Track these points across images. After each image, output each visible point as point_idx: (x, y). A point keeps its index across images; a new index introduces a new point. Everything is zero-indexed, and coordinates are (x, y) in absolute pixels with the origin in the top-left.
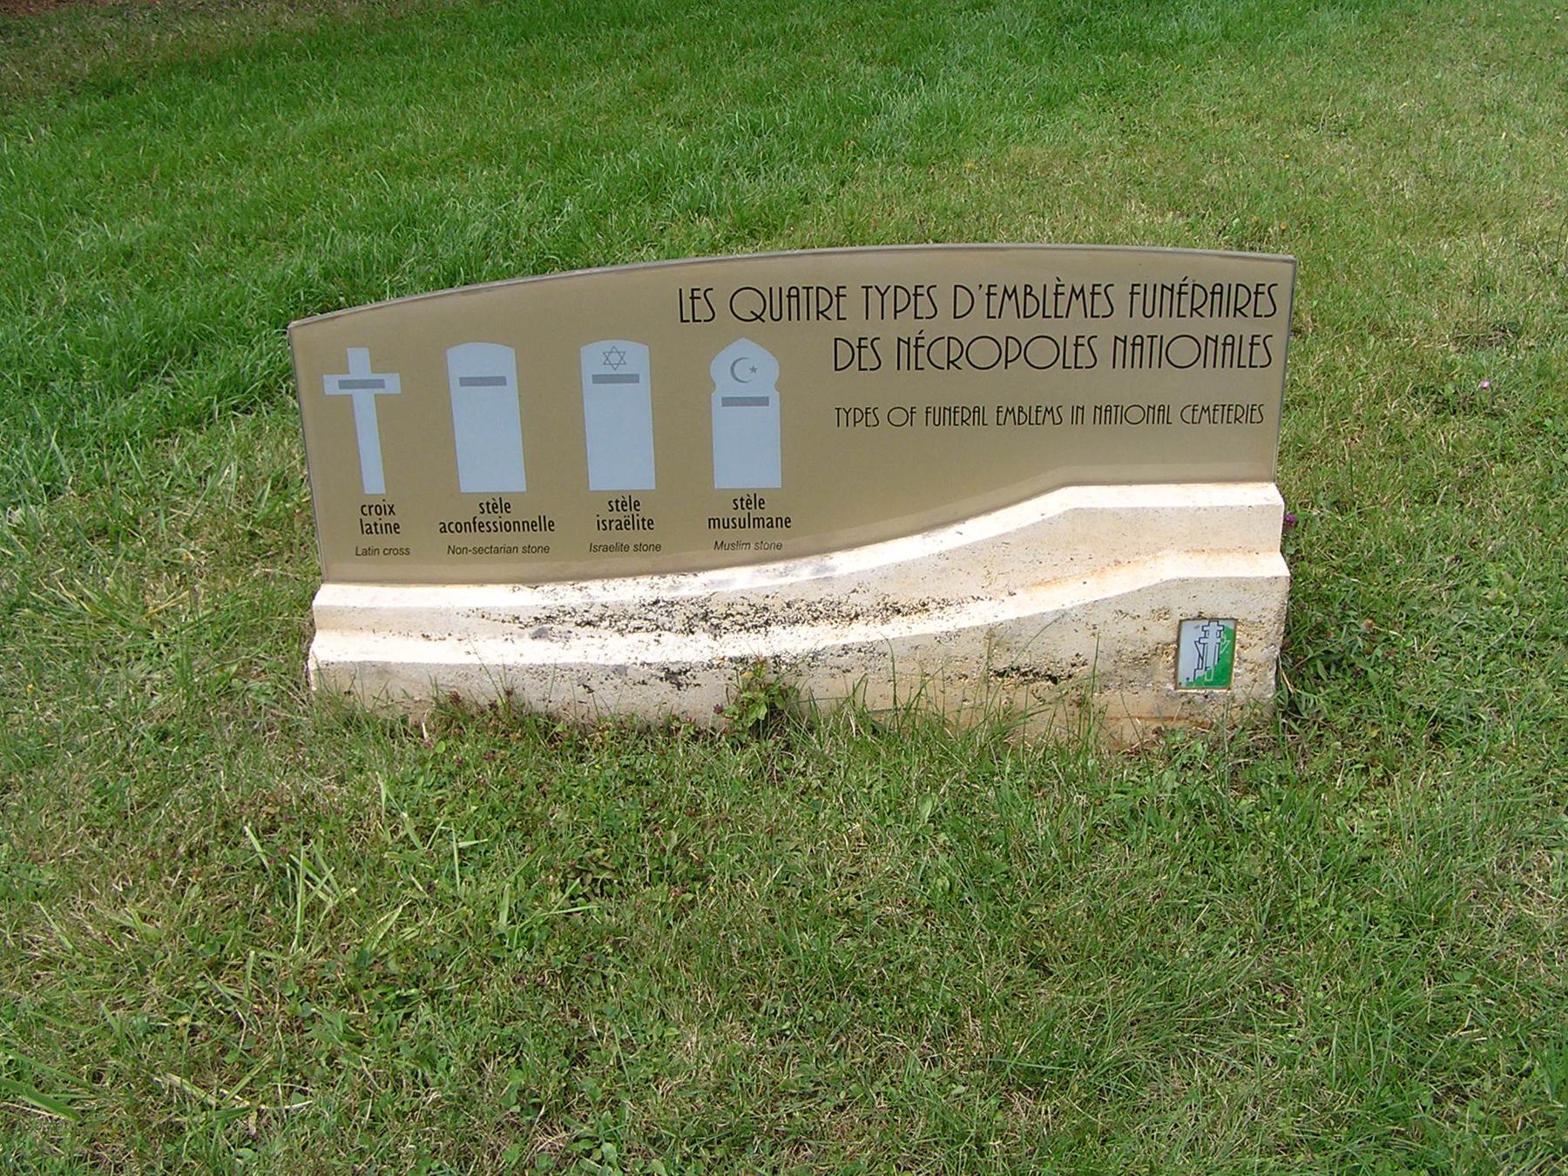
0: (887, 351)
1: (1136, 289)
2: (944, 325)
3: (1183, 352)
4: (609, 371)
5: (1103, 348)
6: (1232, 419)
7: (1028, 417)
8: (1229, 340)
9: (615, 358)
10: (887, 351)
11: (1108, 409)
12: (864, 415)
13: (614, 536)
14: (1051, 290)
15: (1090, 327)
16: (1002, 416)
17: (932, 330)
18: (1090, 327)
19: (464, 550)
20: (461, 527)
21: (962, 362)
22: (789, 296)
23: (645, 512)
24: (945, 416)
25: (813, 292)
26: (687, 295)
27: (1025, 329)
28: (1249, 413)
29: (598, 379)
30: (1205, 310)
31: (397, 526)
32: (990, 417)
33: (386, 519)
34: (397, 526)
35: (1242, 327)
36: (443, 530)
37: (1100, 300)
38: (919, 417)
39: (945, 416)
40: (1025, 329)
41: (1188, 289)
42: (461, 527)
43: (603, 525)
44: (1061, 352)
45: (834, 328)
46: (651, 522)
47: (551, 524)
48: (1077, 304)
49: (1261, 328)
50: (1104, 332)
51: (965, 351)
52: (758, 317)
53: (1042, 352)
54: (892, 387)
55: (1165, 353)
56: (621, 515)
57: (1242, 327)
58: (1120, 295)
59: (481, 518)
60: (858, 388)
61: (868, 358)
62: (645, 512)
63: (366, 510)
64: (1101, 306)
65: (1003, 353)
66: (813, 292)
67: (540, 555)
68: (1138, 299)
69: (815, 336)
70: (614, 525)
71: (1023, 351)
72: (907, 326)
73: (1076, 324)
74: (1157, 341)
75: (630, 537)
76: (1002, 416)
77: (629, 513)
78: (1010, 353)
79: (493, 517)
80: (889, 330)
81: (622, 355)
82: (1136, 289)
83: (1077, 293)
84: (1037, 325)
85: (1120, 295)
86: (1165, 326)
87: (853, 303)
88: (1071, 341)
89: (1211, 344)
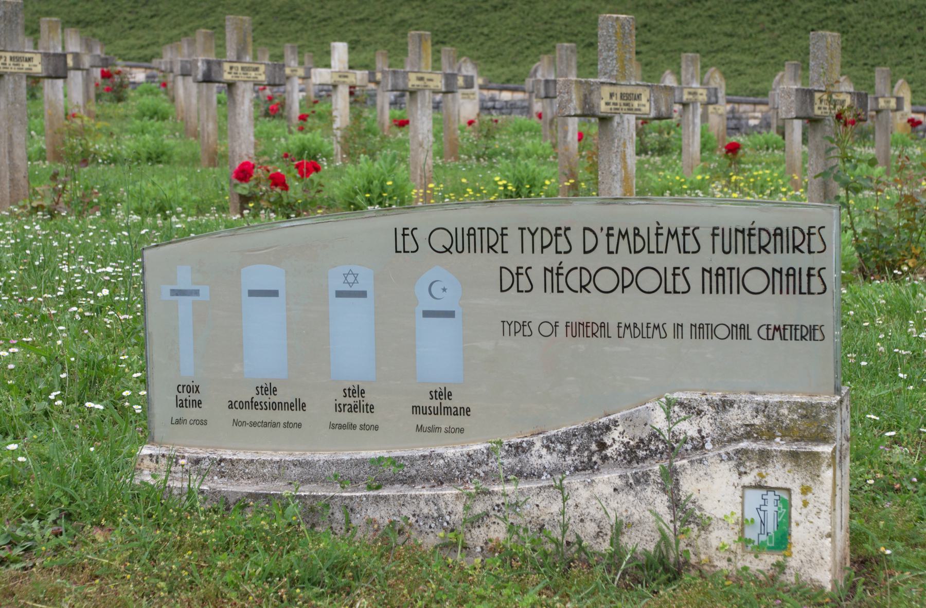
0: (537, 275)
1: (716, 232)
2: (576, 258)
3: (756, 281)
4: (346, 288)
5: (694, 276)
6: (799, 337)
7: (641, 333)
8: (791, 272)
9: (351, 279)
10: (537, 275)
11: (701, 327)
12: (521, 328)
13: (346, 417)
14: (653, 232)
15: (682, 260)
16: (621, 330)
17: (568, 262)
18: (682, 260)
19: (243, 423)
20: (243, 405)
21: (591, 287)
22: (469, 235)
23: (369, 399)
24: (581, 329)
25: (485, 232)
26: (400, 232)
27: (635, 262)
28: (810, 332)
29: (339, 294)
30: (808, 337)
31: (200, 403)
32: (613, 331)
33: (194, 396)
34: (200, 403)
35: (800, 261)
36: (231, 407)
37: (690, 240)
38: (561, 329)
39: (581, 329)
40: (635, 262)
41: (756, 232)
42: (243, 405)
43: (339, 408)
44: (663, 280)
45: (497, 260)
46: (372, 407)
47: (304, 405)
48: (673, 243)
49: (815, 261)
50: (694, 265)
51: (593, 278)
52: (448, 250)
53: (649, 280)
54: (540, 306)
55: (742, 282)
56: (351, 401)
57: (800, 261)
58: (704, 237)
59: (258, 399)
60: (517, 306)
61: (524, 283)
62: (369, 399)
63: (181, 388)
64: (691, 245)
65: (620, 280)
66: (485, 232)
67: (458, 435)
68: (718, 240)
69: (486, 264)
70: (347, 408)
71: (635, 279)
72: (550, 259)
73: (672, 258)
74: (735, 273)
75: (358, 418)
76: (621, 330)
77: (357, 399)
78: (626, 281)
79: (264, 398)
80: (539, 262)
81: (356, 276)
82: (716, 232)
83: (672, 234)
84: (644, 259)
85: (704, 237)
86: (741, 261)
87: (512, 241)
88: (670, 272)
89: (777, 275)
